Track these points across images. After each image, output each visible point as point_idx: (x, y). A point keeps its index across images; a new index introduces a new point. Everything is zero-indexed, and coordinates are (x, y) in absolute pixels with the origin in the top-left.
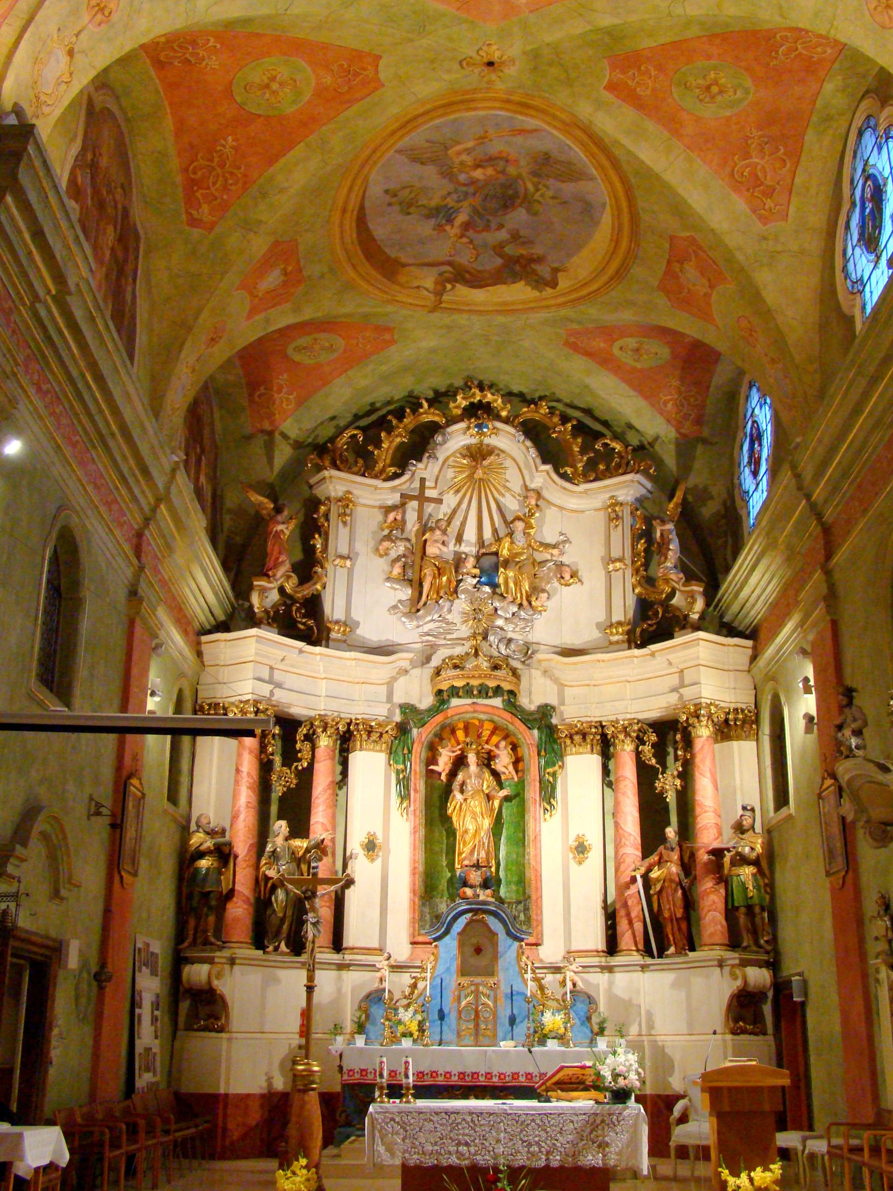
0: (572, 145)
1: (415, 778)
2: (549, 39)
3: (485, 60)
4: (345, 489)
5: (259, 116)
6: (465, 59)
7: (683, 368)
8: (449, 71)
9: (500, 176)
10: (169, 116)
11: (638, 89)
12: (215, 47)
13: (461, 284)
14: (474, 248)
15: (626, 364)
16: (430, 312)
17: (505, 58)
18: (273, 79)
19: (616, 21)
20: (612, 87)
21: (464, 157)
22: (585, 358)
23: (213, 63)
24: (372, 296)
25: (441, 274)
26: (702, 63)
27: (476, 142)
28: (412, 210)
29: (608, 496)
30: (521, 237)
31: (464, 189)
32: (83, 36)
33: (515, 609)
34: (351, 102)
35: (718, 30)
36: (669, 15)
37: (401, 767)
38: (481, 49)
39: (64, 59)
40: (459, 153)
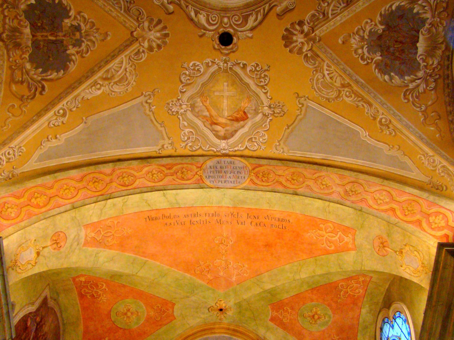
2: (245, 297)
3: (219, 308)
5: (121, 328)
6: (210, 307)
8: (204, 313)
10: (82, 324)
11: (284, 320)
12: (106, 289)
17: (227, 307)
18: (129, 310)
19: (272, 286)
20: (272, 320)
23: (104, 298)
26: (309, 304)
32: (45, 249)
34: (161, 325)
35: (314, 286)
36: (294, 280)
38: (217, 303)
39: (34, 255)
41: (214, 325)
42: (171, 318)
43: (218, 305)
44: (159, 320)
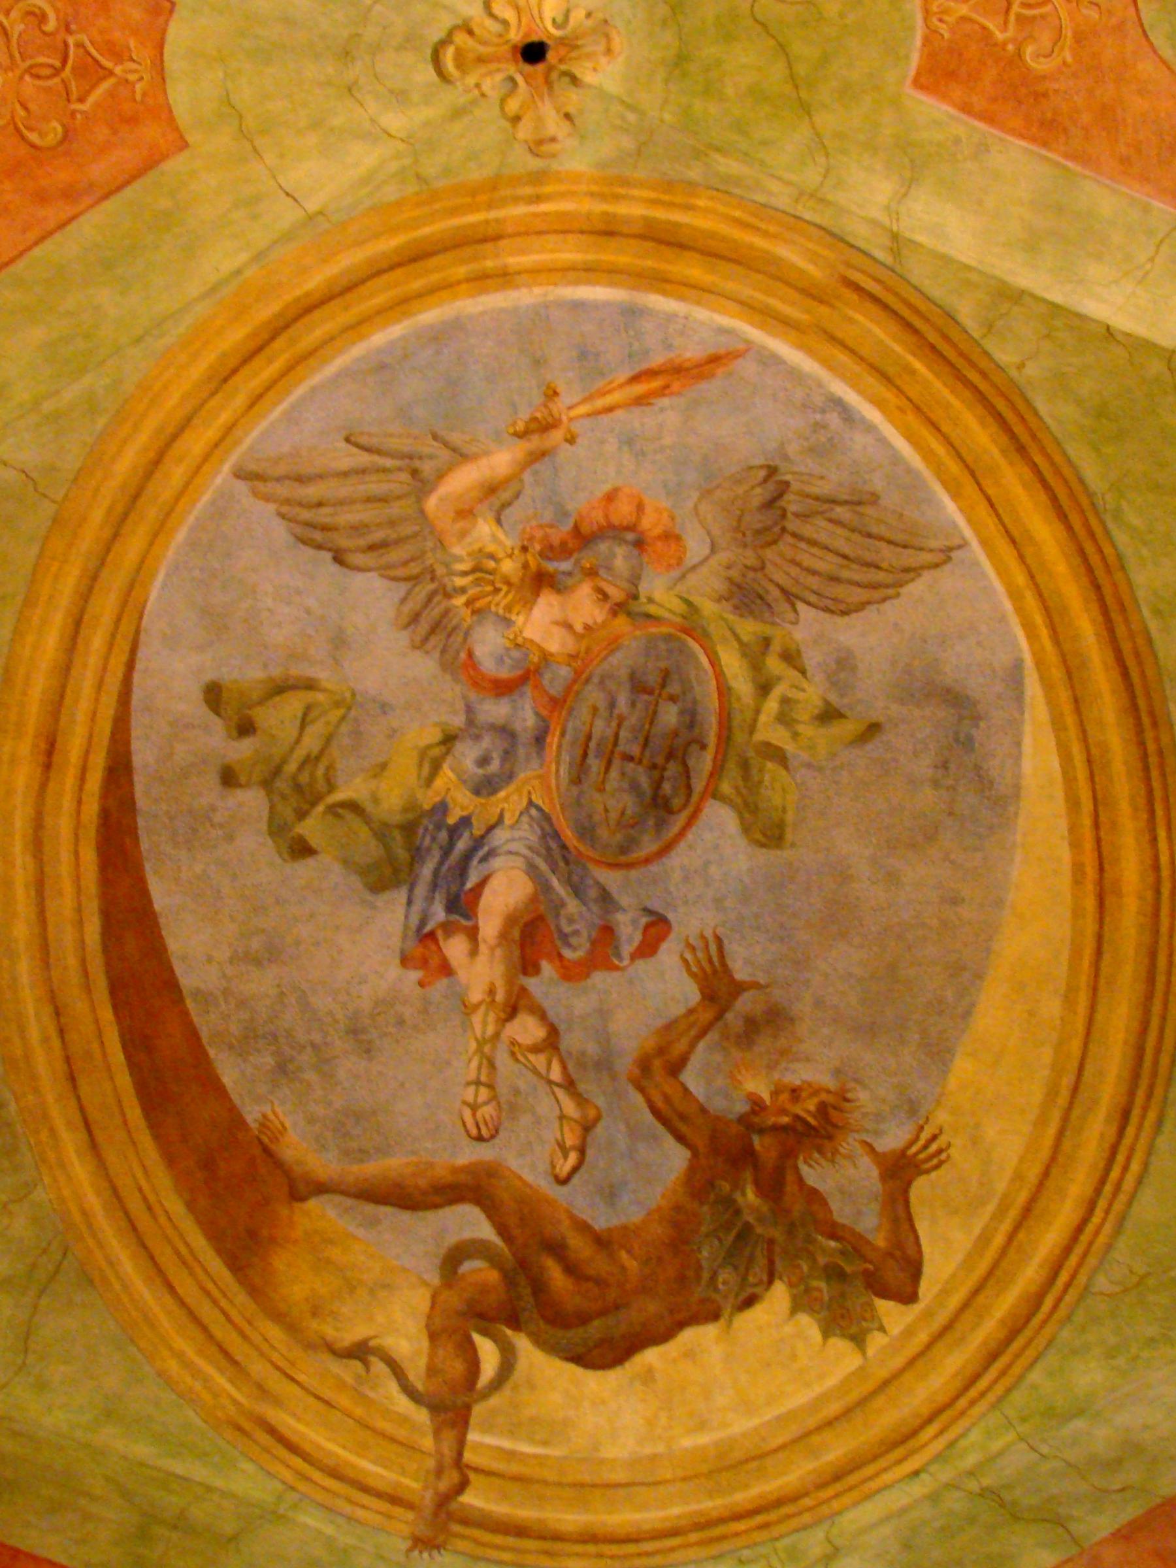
0: (851, 397)
3: (516, 36)
8: (400, 97)
9: (621, 623)
11: (1029, 51)
13: (539, 1342)
14: (570, 1085)
16: (422, 1543)
17: (578, 16)
21: (484, 530)
24: (173, 1366)
25: (454, 1258)
27: (521, 448)
28: (311, 828)
30: (739, 988)
31: (495, 710)
40: (465, 513)
41: (490, 206)
42: (151, 132)
43: (509, 15)
44: (51, 140)
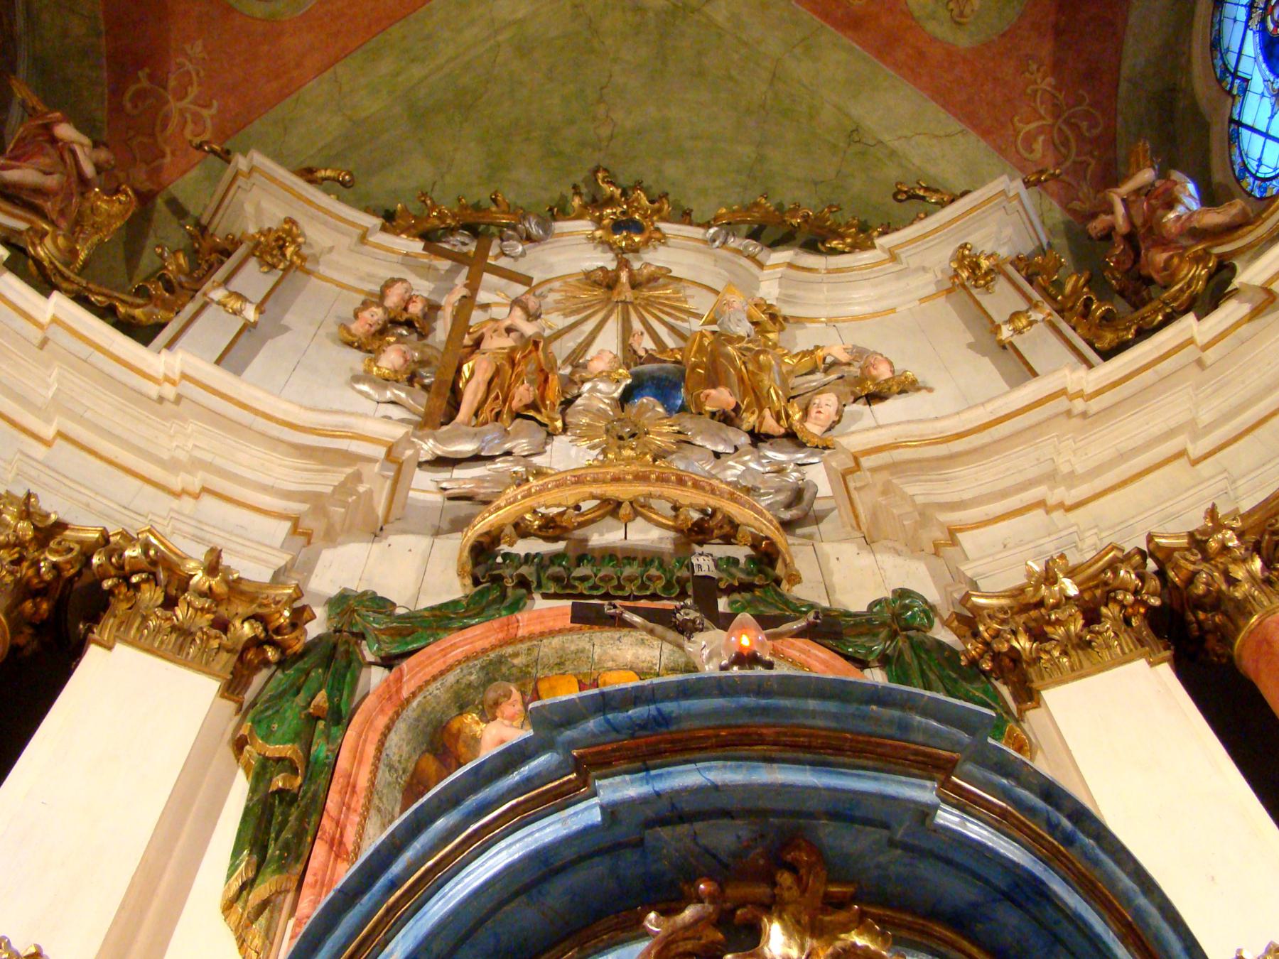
1: (345, 806)
4: (283, 216)
7: (1058, 32)
15: (934, 40)
22: (845, 40)
29: (949, 251)
33: (744, 440)
37: (287, 750)
